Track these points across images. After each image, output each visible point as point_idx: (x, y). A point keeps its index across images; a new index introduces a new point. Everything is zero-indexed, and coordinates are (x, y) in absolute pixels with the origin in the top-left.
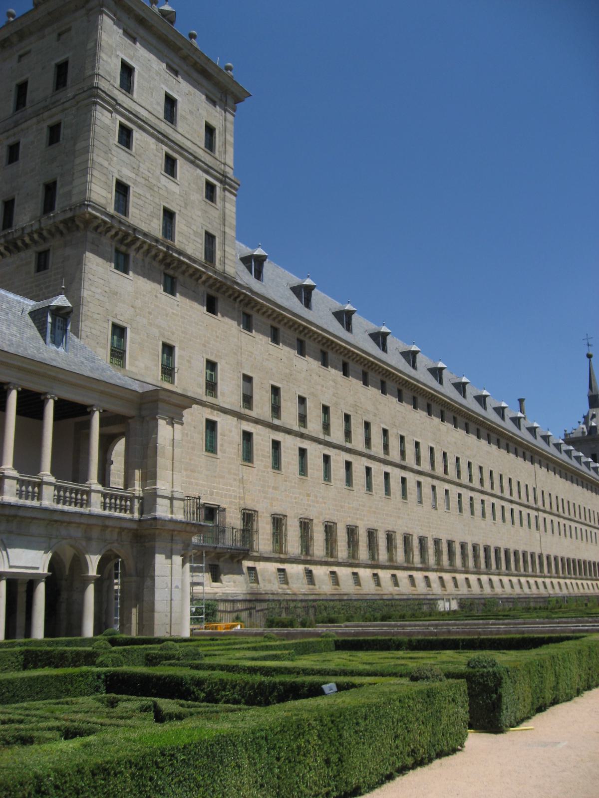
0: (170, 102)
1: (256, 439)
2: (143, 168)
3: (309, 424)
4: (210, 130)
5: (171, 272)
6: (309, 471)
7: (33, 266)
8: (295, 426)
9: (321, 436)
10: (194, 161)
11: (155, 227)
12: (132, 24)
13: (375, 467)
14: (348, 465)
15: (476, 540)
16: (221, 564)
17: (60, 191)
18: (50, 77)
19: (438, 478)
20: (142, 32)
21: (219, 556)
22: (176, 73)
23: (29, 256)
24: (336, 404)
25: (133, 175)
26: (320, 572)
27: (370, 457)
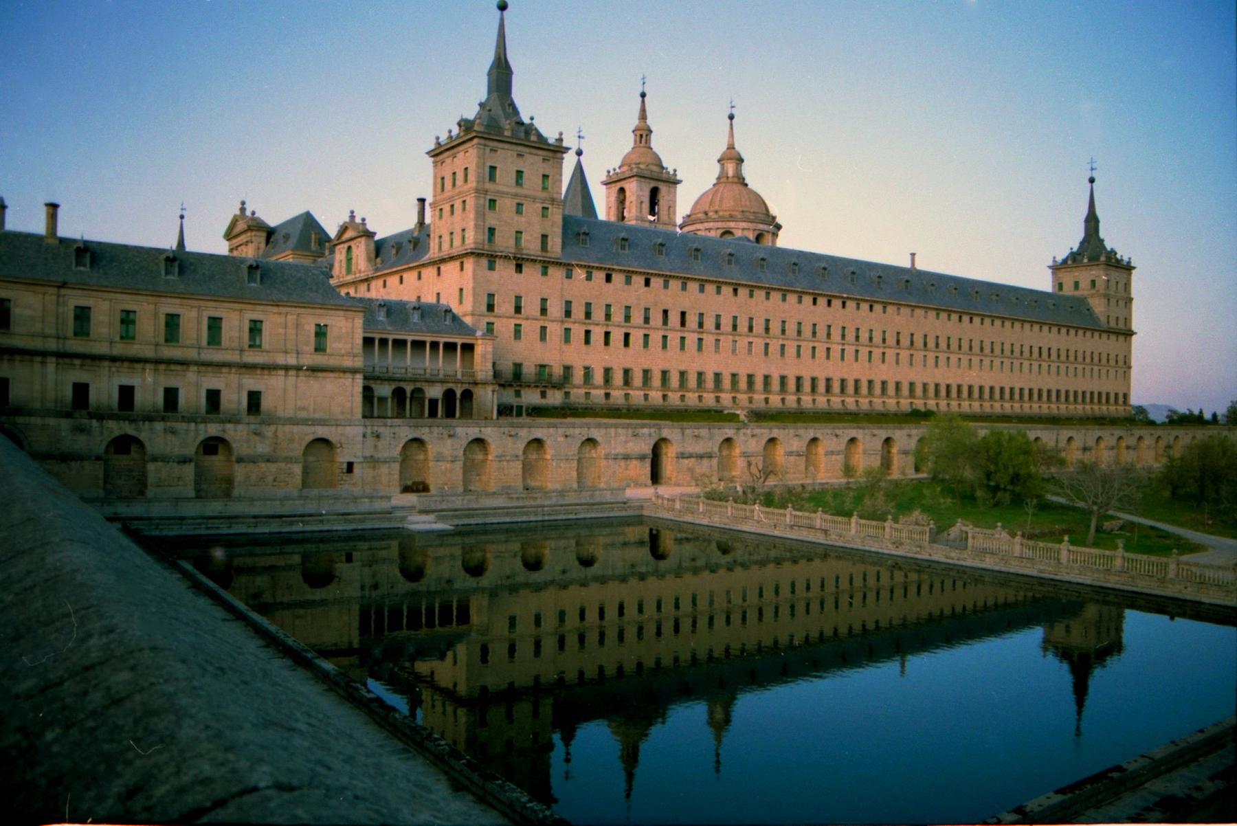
4: (545, 177)
10: (534, 199)
11: (512, 242)
20: (501, 145)
23: (457, 263)
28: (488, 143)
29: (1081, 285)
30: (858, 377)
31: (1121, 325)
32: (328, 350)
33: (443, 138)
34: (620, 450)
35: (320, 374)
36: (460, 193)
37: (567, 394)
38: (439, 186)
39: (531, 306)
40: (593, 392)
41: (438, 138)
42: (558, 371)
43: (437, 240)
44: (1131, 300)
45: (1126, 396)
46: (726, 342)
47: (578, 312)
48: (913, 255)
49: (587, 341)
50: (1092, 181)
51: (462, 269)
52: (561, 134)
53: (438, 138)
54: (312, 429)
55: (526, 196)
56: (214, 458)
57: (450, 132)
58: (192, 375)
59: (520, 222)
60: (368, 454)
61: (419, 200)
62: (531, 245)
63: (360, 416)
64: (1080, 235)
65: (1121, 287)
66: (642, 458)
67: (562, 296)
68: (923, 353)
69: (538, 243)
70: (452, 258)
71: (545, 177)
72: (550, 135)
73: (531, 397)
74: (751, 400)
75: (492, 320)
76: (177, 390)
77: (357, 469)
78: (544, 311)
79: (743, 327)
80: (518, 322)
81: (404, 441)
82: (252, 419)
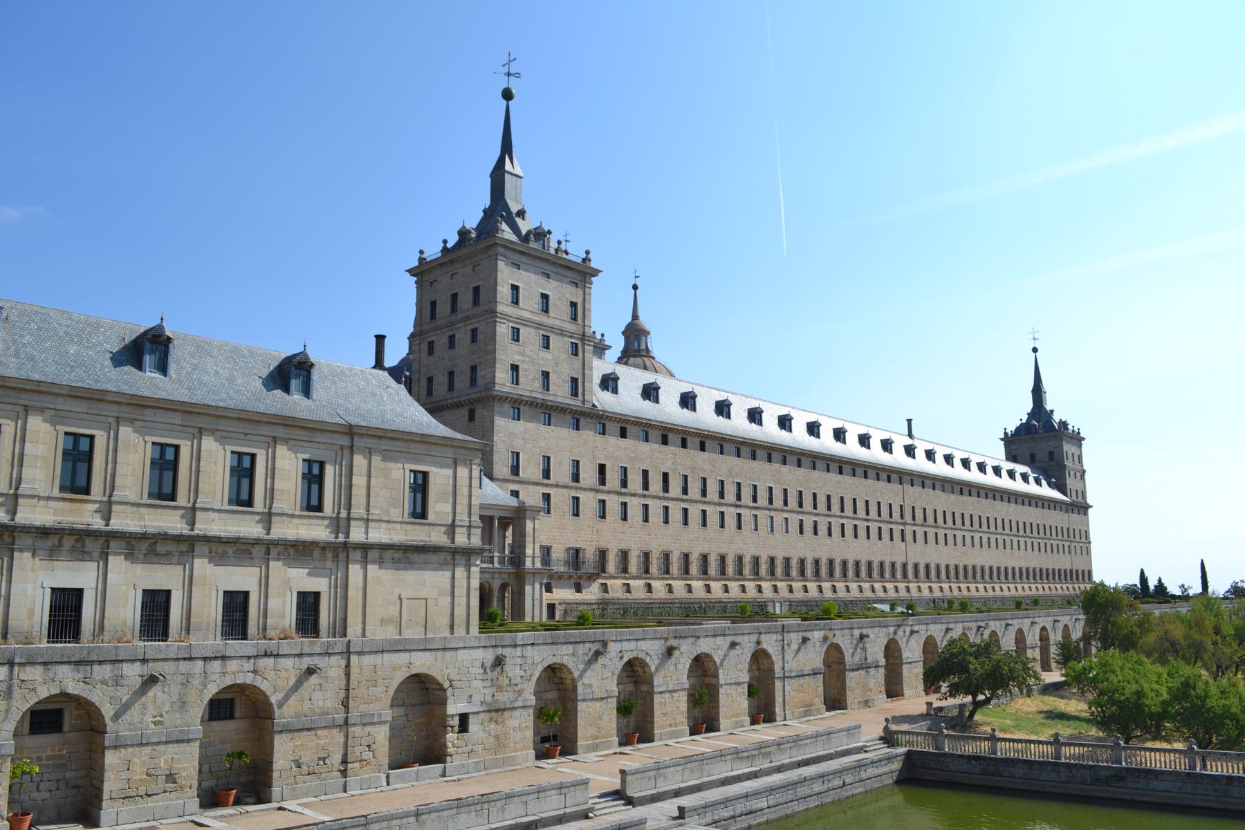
0: (545, 297)
1: (607, 504)
2: (527, 351)
3: (650, 488)
4: (573, 305)
5: (548, 412)
6: (650, 519)
7: (467, 418)
8: (640, 491)
9: (661, 494)
10: (562, 333)
12: (516, 257)
13: (709, 509)
14: (685, 510)
15: (817, 555)
16: (583, 583)
17: (480, 374)
18: (470, 294)
19: (776, 510)
20: (524, 259)
21: (580, 578)
22: (548, 276)
23: (465, 412)
24: (675, 470)
25: (520, 358)
26: (657, 584)
27: (705, 503)
28: (509, 254)
29: (1037, 458)
30: (884, 558)
31: (1080, 499)
32: (431, 517)
33: (433, 251)
34: (792, 665)
35: (415, 557)
36: (468, 318)
37: (605, 588)
38: (427, 313)
39: (561, 472)
40: (632, 583)
41: (421, 252)
42: (590, 555)
43: (424, 382)
44: (1084, 472)
45: (1090, 573)
46: (763, 516)
47: (613, 479)
48: (909, 421)
49: (625, 518)
50: (1035, 350)
51: (472, 418)
52: (587, 252)
53: (421, 252)
54: (403, 658)
55: (552, 328)
56: (229, 725)
57: (445, 242)
58: (202, 566)
59: (546, 359)
60: (489, 698)
61: (377, 337)
62: (560, 393)
63: (475, 629)
64: (1029, 406)
65: (1076, 458)
66: (815, 673)
67: (595, 458)
68: (935, 530)
69: (567, 388)
70: (456, 406)
71: (573, 305)
72: (575, 253)
73: (563, 594)
74: (791, 591)
75: (515, 487)
76: (169, 592)
77: (473, 725)
78: (576, 478)
79: (778, 502)
80: (546, 491)
81: (540, 668)
82: (306, 643)
